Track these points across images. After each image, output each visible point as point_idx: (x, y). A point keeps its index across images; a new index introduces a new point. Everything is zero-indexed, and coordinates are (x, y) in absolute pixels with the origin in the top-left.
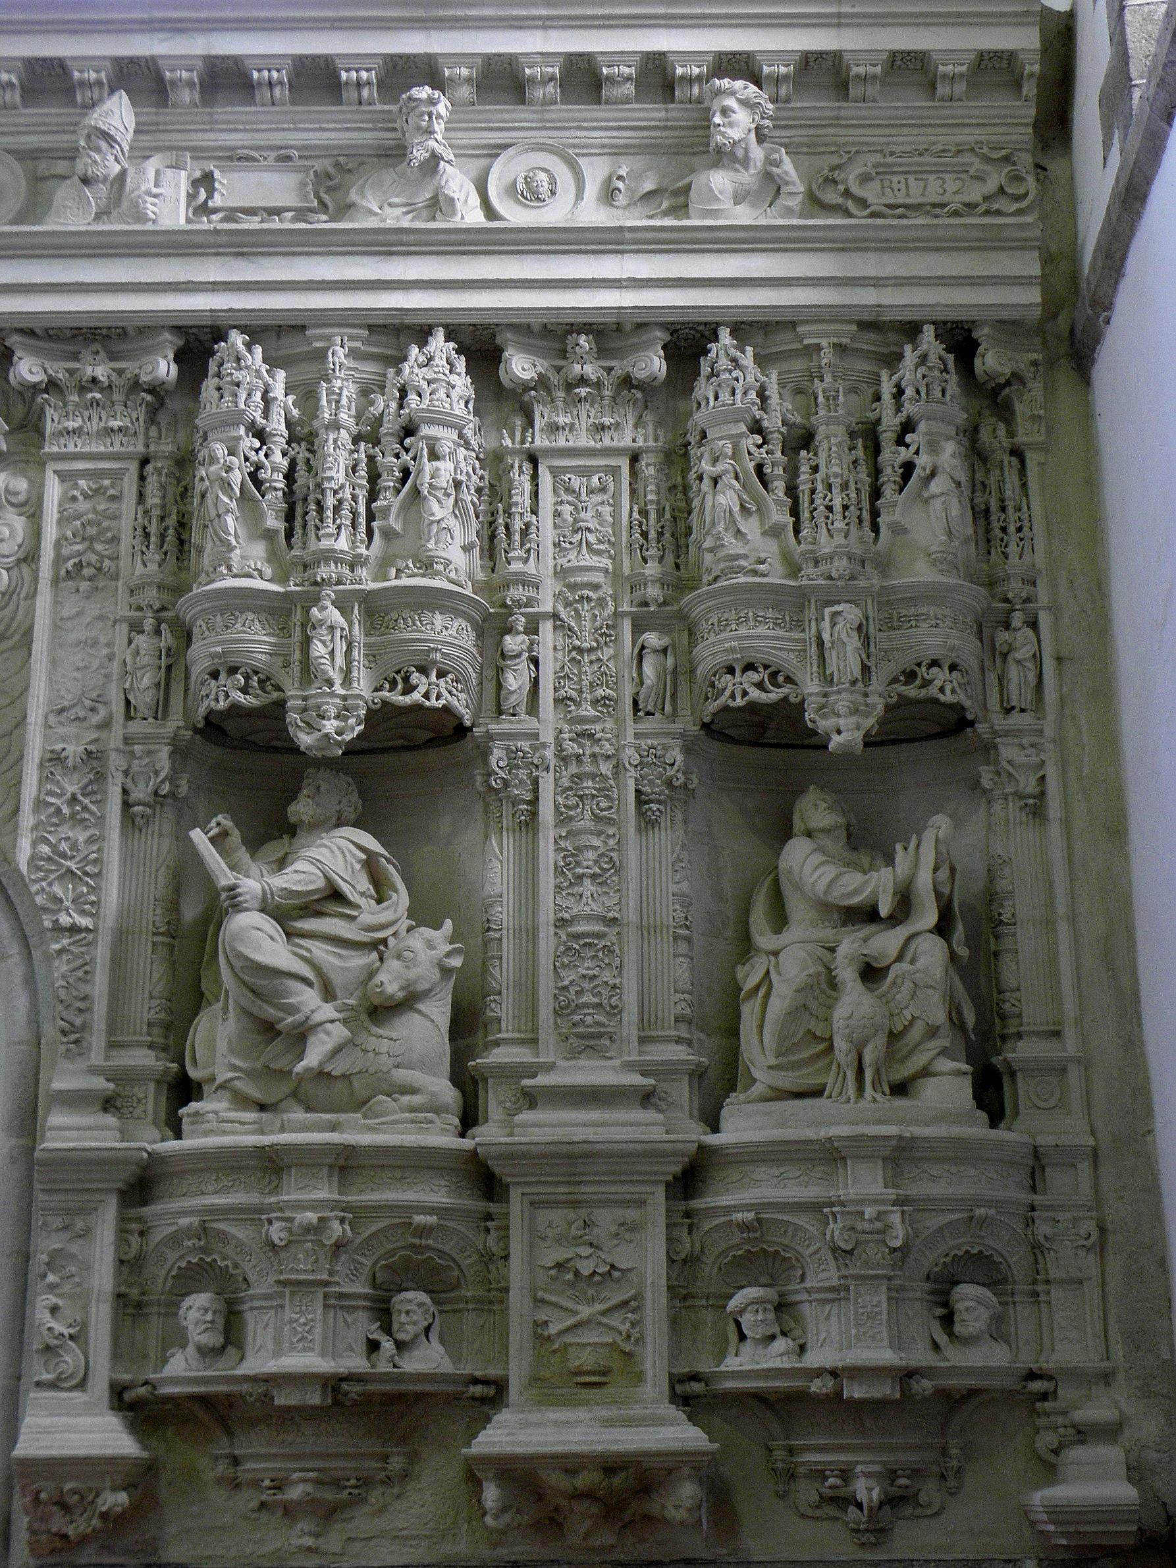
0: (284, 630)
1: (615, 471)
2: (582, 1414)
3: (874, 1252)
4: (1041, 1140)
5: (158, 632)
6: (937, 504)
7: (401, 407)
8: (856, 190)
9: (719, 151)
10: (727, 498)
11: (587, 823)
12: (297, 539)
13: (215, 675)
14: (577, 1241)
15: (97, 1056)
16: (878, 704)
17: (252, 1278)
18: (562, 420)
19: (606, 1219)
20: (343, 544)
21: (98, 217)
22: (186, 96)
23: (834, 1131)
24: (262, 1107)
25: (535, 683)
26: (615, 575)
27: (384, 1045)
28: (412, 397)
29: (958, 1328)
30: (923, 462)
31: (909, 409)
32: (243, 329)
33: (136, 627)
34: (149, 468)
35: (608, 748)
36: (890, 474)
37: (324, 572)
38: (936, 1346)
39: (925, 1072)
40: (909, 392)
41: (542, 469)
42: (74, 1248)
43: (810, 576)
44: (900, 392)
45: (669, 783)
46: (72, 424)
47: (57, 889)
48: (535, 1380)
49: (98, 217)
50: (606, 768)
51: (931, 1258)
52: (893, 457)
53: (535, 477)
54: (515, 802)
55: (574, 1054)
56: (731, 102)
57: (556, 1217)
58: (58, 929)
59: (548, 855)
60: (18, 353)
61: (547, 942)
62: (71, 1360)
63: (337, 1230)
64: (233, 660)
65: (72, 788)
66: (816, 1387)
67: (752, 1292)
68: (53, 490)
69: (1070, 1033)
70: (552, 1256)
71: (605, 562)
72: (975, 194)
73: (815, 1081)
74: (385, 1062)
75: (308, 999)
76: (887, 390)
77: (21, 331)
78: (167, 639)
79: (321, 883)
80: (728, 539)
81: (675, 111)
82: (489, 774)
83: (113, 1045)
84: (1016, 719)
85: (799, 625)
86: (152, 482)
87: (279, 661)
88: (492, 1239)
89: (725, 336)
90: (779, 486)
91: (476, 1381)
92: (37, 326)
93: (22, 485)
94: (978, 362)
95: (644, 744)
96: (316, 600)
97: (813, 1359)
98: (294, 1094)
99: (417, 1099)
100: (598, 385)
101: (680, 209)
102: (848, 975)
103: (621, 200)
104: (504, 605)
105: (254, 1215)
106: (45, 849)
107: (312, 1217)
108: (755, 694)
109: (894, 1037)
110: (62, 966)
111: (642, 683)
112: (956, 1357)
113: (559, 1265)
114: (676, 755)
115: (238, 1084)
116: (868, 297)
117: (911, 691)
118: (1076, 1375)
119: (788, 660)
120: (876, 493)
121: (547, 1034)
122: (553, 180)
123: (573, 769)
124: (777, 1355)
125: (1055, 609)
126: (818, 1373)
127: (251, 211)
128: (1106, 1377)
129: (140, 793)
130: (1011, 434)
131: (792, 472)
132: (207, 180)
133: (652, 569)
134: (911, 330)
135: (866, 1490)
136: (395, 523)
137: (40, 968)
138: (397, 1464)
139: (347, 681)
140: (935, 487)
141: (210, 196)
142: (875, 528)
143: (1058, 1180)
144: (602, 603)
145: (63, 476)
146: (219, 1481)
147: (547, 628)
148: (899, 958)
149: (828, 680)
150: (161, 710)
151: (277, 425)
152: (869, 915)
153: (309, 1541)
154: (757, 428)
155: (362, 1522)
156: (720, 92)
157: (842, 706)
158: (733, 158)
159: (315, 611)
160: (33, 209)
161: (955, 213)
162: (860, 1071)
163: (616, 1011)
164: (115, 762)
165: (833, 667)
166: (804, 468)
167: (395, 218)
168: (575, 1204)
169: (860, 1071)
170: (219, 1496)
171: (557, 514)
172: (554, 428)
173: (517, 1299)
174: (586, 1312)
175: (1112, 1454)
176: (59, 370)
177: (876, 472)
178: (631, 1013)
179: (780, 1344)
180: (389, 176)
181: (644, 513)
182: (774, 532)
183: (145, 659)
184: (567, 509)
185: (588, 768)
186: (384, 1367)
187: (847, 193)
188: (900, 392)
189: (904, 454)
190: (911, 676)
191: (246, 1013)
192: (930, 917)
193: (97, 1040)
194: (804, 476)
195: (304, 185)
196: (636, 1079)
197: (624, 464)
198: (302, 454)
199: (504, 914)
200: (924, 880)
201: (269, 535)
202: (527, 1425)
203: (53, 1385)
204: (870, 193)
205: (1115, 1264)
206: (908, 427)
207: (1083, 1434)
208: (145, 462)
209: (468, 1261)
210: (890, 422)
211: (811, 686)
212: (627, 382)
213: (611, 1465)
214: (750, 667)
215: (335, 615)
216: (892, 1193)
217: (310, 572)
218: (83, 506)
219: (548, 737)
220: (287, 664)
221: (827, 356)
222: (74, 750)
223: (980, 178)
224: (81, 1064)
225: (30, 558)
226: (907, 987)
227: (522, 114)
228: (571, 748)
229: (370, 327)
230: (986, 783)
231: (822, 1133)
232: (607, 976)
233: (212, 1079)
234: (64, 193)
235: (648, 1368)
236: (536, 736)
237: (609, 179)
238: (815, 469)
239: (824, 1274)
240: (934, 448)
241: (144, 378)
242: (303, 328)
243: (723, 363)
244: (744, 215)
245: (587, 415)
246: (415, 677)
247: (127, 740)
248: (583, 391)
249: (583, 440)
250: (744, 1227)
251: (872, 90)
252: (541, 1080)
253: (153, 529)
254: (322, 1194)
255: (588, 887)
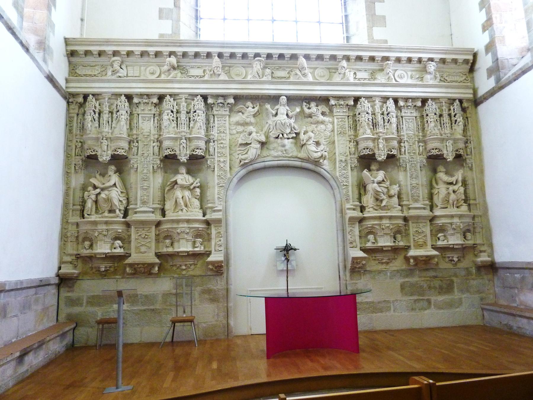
0: (374, 143)
1: (413, 119)
2: (421, 250)
3: (458, 229)
4: (475, 214)
5: (354, 142)
6: (460, 126)
7: (387, 110)
8: (446, 78)
9: (429, 72)
10: (432, 124)
11: (413, 170)
12: (375, 129)
13: (364, 149)
14: (418, 228)
15: (351, 203)
16: (454, 154)
17: (378, 233)
18: (406, 111)
19: (421, 224)
20: (382, 131)
21: (342, 79)
22: (353, 61)
23: (453, 213)
24: (376, 210)
25: (405, 150)
26: (414, 135)
27: (392, 202)
28: (388, 108)
29: (467, 238)
30: (458, 120)
31: (456, 112)
32: (364, 97)
33: (350, 142)
34: (349, 117)
35: (415, 160)
36: (453, 122)
37: (381, 135)
38: (464, 241)
39: (461, 205)
40: (456, 109)
41: (403, 119)
42: (352, 229)
43: (444, 136)
44: (454, 110)
45: (424, 165)
46: (339, 111)
47: (343, 179)
48: (414, 246)
49: (342, 79)
50: (415, 162)
51: (463, 230)
52: (453, 119)
53: (402, 120)
54: (403, 167)
55: (414, 202)
56: (431, 65)
57: (415, 225)
58: (344, 185)
59: (409, 175)
60: (331, 100)
61: (409, 188)
62: (354, 244)
63: (391, 227)
64: (368, 147)
65: (344, 165)
66: (451, 246)
67: (442, 234)
68: (336, 121)
69: (477, 200)
70: (415, 230)
71: (413, 133)
72: (462, 79)
73: (447, 206)
74: (393, 204)
75: (382, 195)
76: (452, 109)
77: (333, 97)
78: (355, 143)
79: (382, 179)
80: (433, 130)
81: (421, 66)
82: (400, 163)
83: (353, 201)
84: (468, 156)
85: (442, 143)
86: (350, 120)
87: (374, 147)
88: (407, 227)
89: (430, 100)
90: (439, 122)
91: (406, 246)
92: (334, 96)
93: (331, 120)
94: (463, 105)
95: (421, 159)
96: (379, 139)
97: (450, 243)
98: (380, 208)
99: (397, 209)
100: (411, 106)
101: (422, 80)
102: (452, 192)
103: (413, 78)
104: (401, 139)
105: (380, 225)
106: (341, 174)
107: (388, 225)
108: (437, 153)
109: (457, 200)
110: (344, 191)
111: (419, 150)
112: (467, 242)
113: (416, 231)
114: (425, 161)
115: (374, 207)
116: (450, 95)
117: (457, 153)
118: (480, 244)
119: (442, 148)
120: (451, 124)
121: (410, 200)
122: (404, 75)
123: (411, 163)
124: (445, 242)
125: (473, 141)
126: (451, 245)
127: (362, 79)
128: (483, 245)
129: (353, 166)
130: (466, 115)
131: (440, 120)
132: (355, 73)
133: (421, 134)
134: (454, 100)
135: (456, 259)
136: (388, 127)
137: (341, 190)
138: (396, 257)
139: (384, 150)
140: (460, 123)
141: (356, 76)
142: (452, 129)
143: (476, 219)
144: (413, 139)
145: (337, 118)
146: (373, 260)
147: (406, 142)
148: (458, 190)
149: (447, 151)
150: (354, 154)
151: (370, 112)
152: (451, 183)
153: (385, 267)
154: (435, 114)
155: (391, 265)
156: (430, 64)
157: (450, 155)
158: (430, 73)
159: (379, 140)
160: (330, 78)
161: (459, 82)
162: (453, 205)
163: (419, 197)
164: (349, 161)
165: (448, 149)
166: (442, 120)
167: (384, 81)
168: (417, 223)
169: (453, 205)
170: (372, 261)
171: (406, 125)
172: (405, 113)
173: (411, 235)
174: (420, 237)
175: (486, 254)
176: (336, 102)
177: (451, 121)
178: (421, 197)
179: (446, 241)
180: (381, 74)
181: (418, 126)
182: (439, 130)
183: (352, 146)
184: (407, 125)
185: (413, 163)
186: (397, 245)
187: (444, 79)
188: (454, 110)
189: (456, 119)
190: (457, 151)
191: (374, 197)
192: (460, 184)
193: (351, 201)
194: (442, 122)
195: (369, 75)
196: (423, 206)
197: (415, 118)
198: (374, 117)
199: (402, 183)
200: (460, 179)
201: (371, 129)
202: (415, 252)
203: (352, 247)
204: (447, 78)
205: (484, 230)
206: (455, 115)
207: (481, 252)
208: (348, 116)
209: (403, 231)
210: (453, 114)
211: (445, 152)
212: (415, 106)
213: (427, 256)
214: (436, 149)
215: (382, 141)
216: (460, 221)
217: (378, 134)
218: (340, 123)
219: (407, 158)
220: (375, 148)
221: (444, 104)
222: (343, 160)
223: (462, 77)
224: (349, 204)
225: (333, 131)
226: (459, 194)
227: (400, 65)
228: (411, 160)
229: (382, 98)
230: (464, 165)
231: (451, 213)
232: (417, 192)
233: (368, 206)
234: (336, 75)
235: (428, 244)
236: (406, 158)
237: (411, 75)
238: (443, 120)
239: (451, 232)
240: (459, 118)
241: (349, 104)
242: (372, 97)
243: (430, 104)
244: (431, 82)
245: (409, 111)
246: (392, 150)
247: (350, 158)
248: (409, 107)
249: (409, 115)
250: (440, 226)
251: (449, 64)
252: (410, 206)
253: (352, 127)
254: (388, 222)
255: (414, 179)
